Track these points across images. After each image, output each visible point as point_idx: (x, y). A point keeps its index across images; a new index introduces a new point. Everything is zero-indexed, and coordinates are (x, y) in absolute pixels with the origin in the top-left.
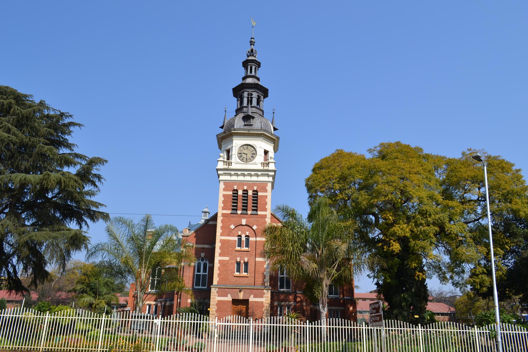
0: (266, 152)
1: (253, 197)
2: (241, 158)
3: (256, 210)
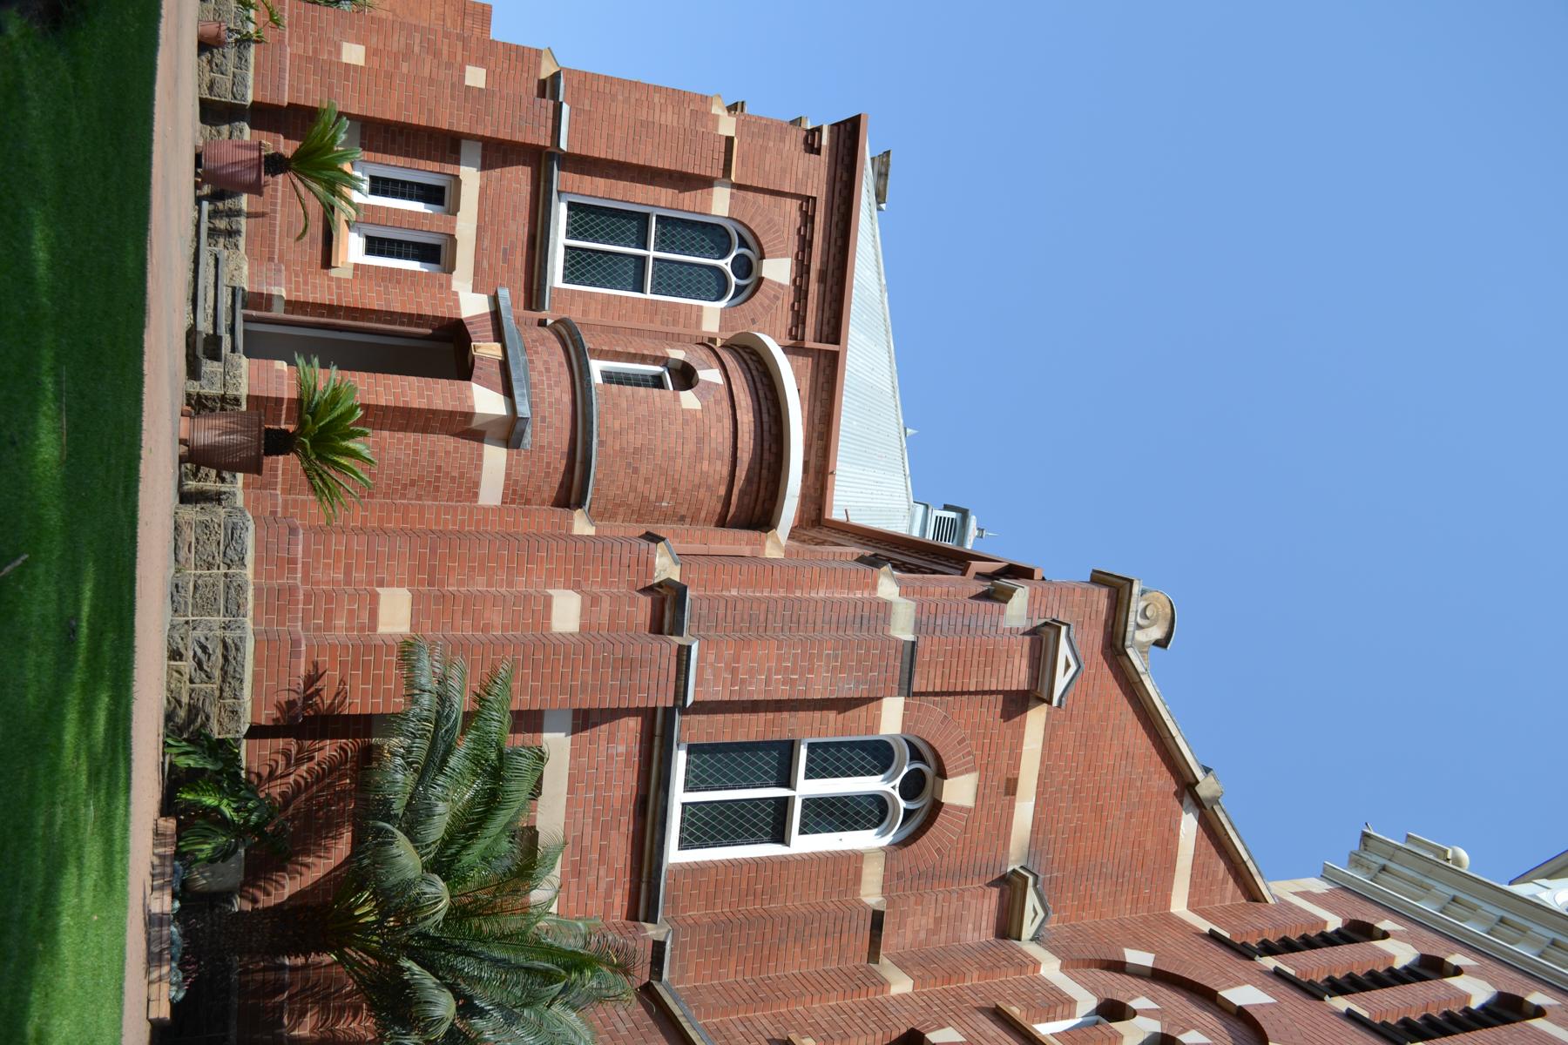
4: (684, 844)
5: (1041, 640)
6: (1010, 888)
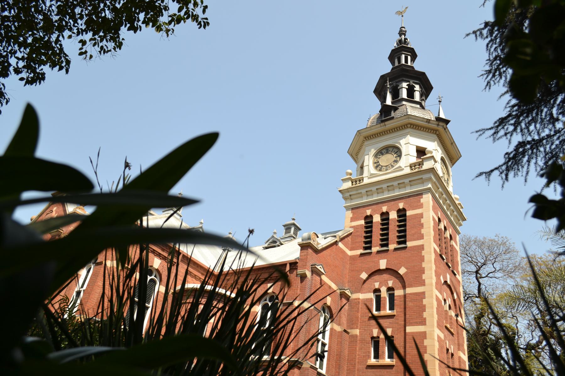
0: (421, 152)
1: (399, 221)
2: (378, 168)
3: (404, 242)
4: (322, 369)
5: (315, 271)
6: (343, 295)
